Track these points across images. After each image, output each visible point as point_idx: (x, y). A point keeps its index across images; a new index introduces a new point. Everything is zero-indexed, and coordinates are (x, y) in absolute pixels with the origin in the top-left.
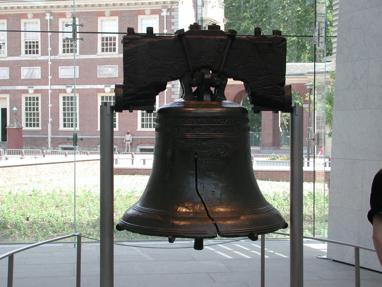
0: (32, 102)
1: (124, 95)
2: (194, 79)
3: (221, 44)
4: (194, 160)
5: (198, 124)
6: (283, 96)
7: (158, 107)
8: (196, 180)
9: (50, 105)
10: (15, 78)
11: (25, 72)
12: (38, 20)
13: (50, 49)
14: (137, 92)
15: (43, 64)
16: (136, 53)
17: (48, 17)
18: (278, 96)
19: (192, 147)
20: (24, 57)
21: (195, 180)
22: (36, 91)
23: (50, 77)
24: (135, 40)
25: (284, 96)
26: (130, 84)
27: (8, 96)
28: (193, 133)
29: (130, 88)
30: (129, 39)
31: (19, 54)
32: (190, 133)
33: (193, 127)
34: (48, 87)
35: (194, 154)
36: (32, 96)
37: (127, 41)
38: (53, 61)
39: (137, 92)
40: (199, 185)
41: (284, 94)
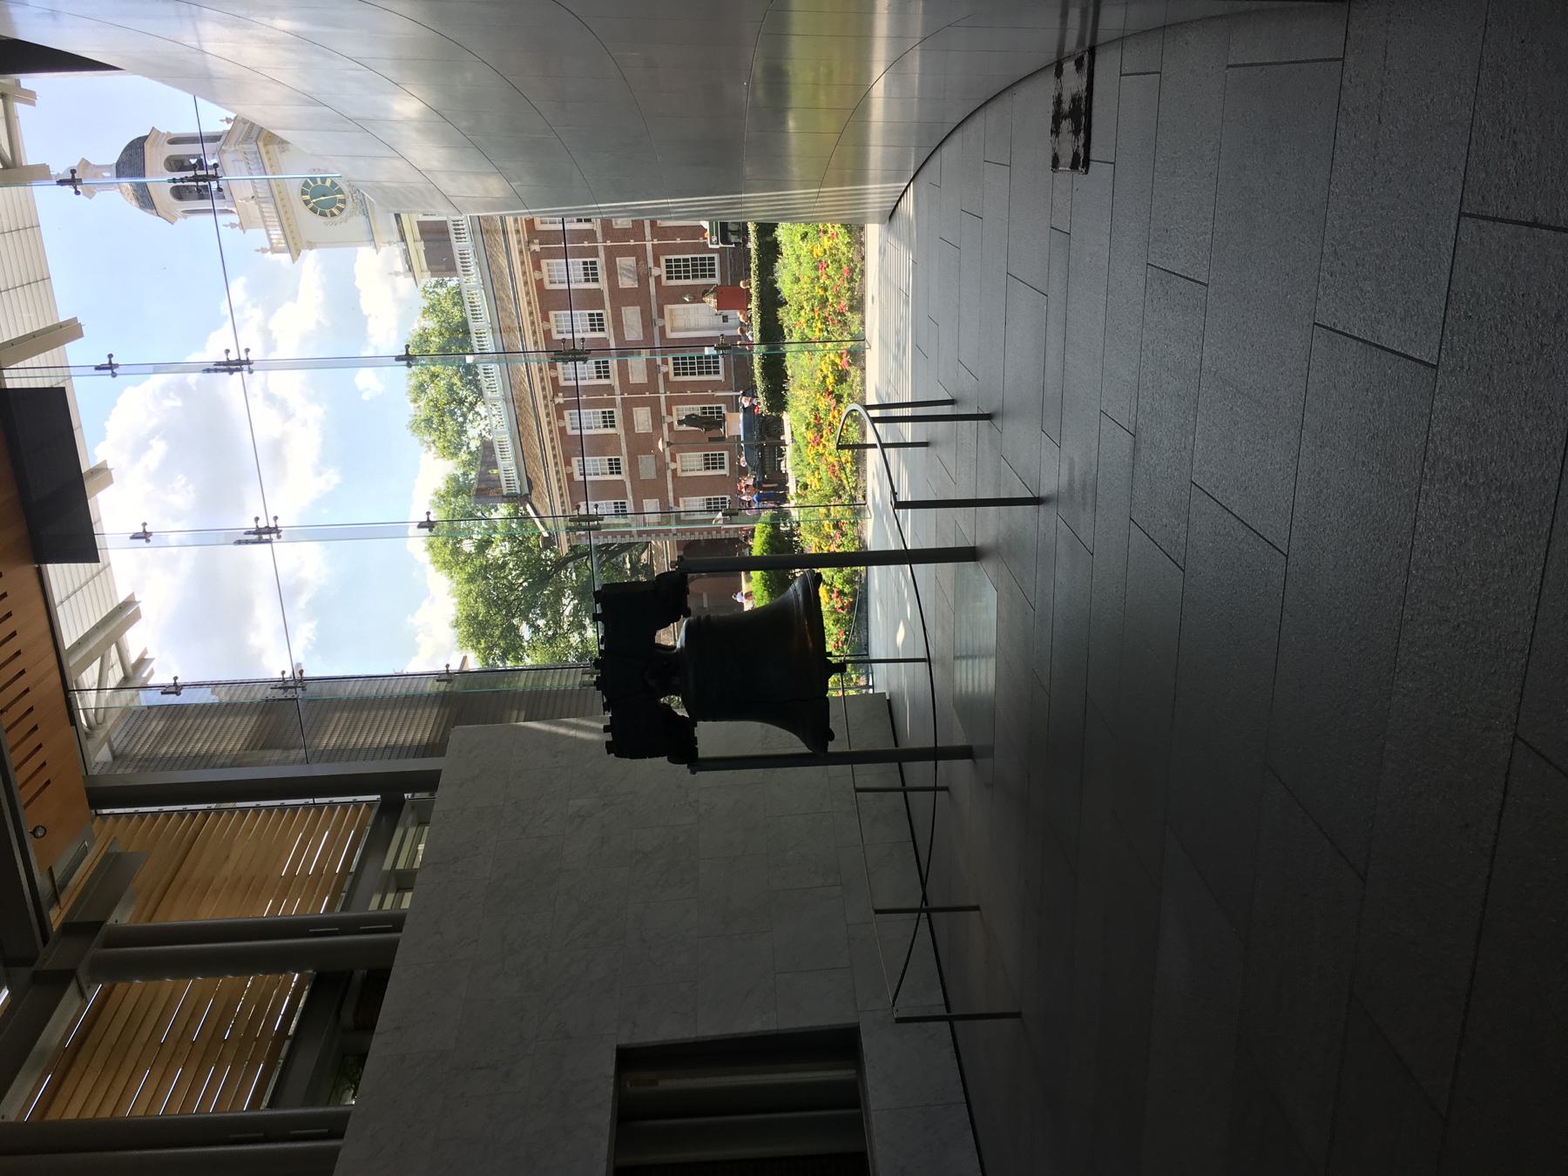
0: (674, 270)
9: (678, 241)
10: (637, 296)
11: (627, 282)
12: (544, 262)
13: (586, 244)
15: (611, 254)
17: (537, 248)
20: (603, 284)
22: (657, 264)
23: (632, 242)
27: (667, 308)
31: (599, 291)
34: (649, 245)
36: (664, 269)
38: (606, 237)
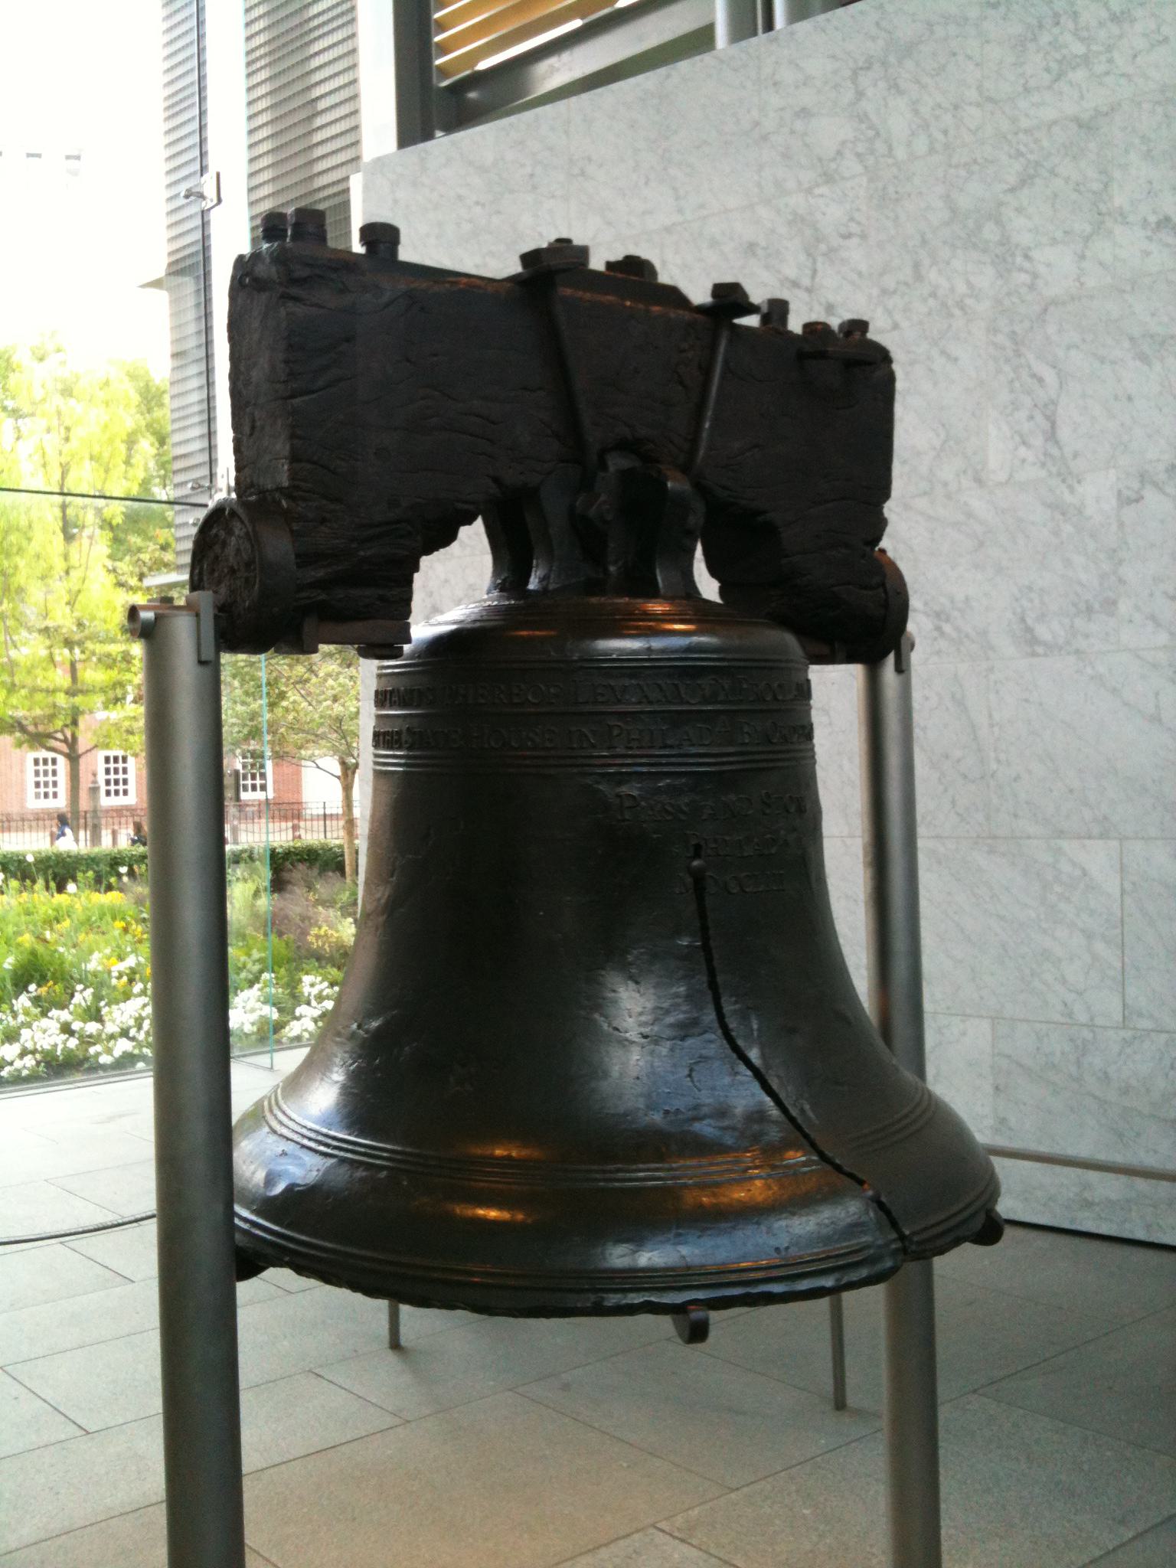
1: (298, 556)
2: (603, 498)
3: (685, 345)
4: (689, 880)
5: (706, 702)
6: (881, 590)
7: (422, 629)
8: (713, 985)
14: (354, 545)
16: (348, 340)
18: (866, 588)
19: (683, 817)
21: (705, 979)
24: (336, 270)
25: (886, 592)
26: (324, 502)
28: (679, 746)
29: (323, 521)
30: (308, 265)
32: (665, 747)
33: (678, 720)
35: (691, 853)
37: (301, 272)
39: (354, 545)
40: (728, 1008)
41: (883, 585)
